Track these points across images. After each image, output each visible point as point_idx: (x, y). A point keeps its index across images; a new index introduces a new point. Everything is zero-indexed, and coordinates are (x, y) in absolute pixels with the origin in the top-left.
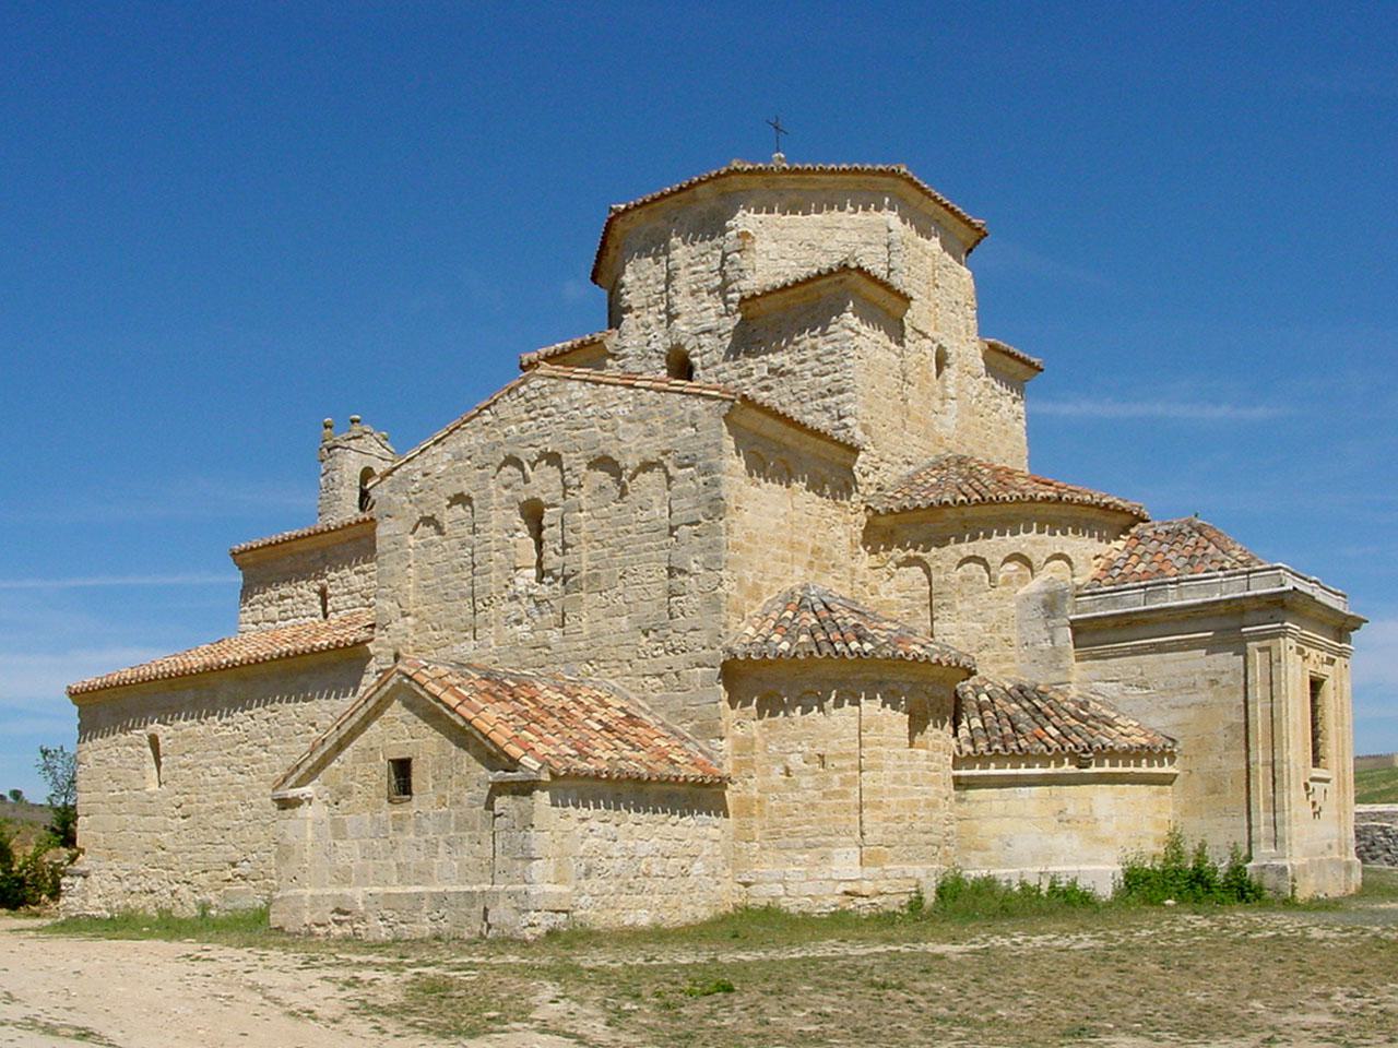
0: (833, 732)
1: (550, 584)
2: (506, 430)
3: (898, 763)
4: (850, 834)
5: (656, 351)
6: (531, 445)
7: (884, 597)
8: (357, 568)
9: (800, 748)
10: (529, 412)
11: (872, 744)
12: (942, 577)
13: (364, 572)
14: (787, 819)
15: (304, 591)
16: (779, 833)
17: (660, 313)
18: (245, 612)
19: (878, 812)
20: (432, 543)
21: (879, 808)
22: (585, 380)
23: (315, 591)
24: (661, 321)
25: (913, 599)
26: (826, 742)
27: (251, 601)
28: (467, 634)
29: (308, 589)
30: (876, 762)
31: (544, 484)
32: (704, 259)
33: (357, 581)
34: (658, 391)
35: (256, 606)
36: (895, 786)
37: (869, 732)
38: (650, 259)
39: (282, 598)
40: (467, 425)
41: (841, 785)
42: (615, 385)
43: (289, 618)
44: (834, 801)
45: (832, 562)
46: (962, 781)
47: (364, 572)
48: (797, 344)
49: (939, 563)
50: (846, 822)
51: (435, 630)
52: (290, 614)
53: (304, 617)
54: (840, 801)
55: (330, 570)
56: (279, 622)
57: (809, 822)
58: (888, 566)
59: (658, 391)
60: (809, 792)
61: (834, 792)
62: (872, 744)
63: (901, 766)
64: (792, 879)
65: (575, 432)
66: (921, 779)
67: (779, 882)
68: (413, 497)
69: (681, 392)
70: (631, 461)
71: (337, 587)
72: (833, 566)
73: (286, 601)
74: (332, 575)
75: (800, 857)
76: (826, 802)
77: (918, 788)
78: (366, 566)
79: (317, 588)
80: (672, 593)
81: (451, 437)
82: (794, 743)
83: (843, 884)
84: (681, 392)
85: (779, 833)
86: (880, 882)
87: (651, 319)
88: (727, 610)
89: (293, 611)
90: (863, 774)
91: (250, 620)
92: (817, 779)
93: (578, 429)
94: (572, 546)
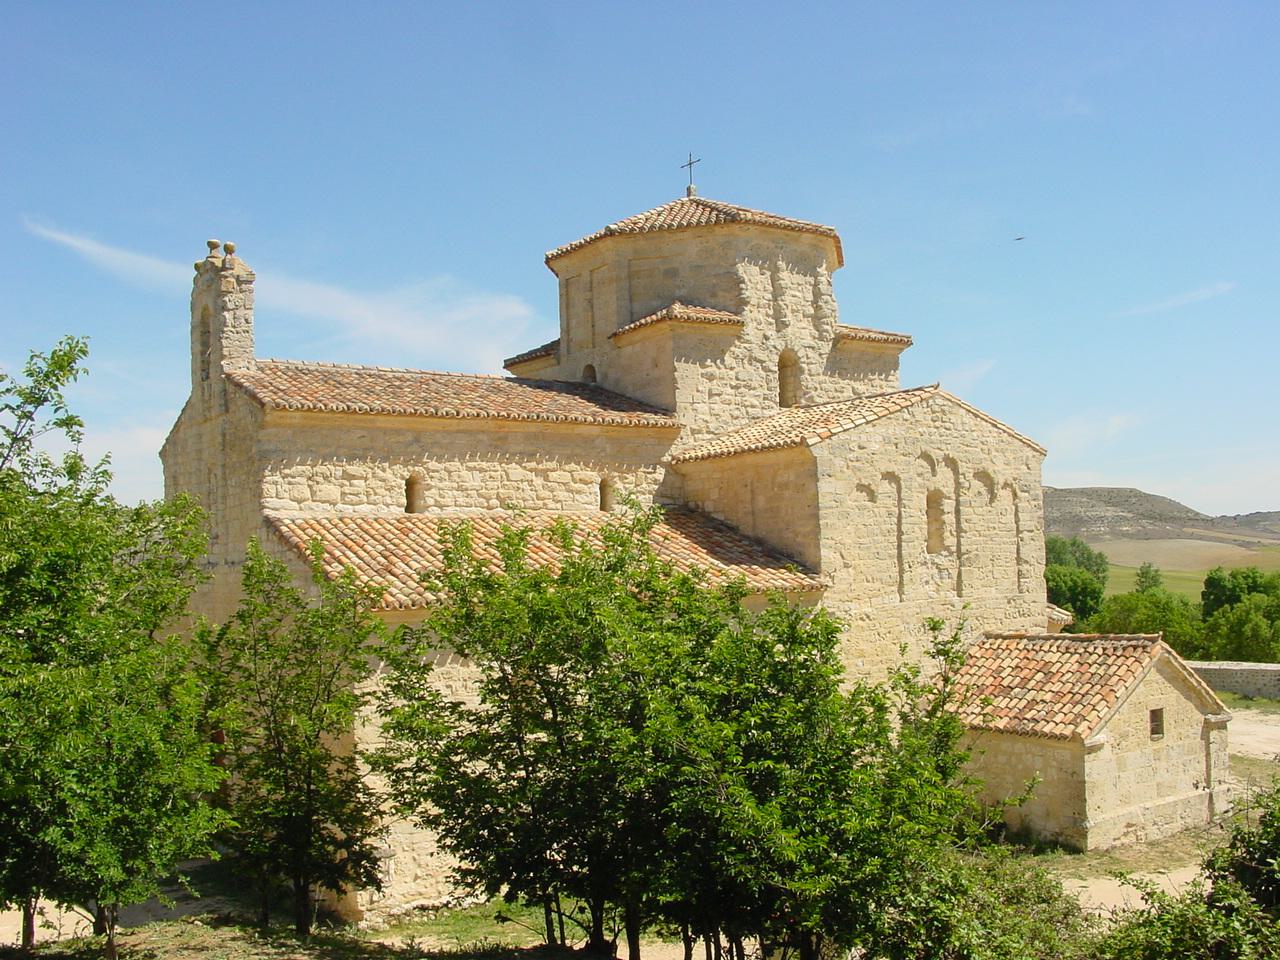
1: (946, 556)
2: (920, 430)
5: (775, 347)
6: (939, 449)
8: (471, 464)
10: (934, 421)
13: (481, 470)
15: (388, 475)
17: (768, 315)
18: (275, 483)
20: (865, 508)
22: (969, 411)
23: (402, 478)
24: (771, 324)
27: (287, 471)
28: (893, 588)
29: (396, 475)
31: (944, 479)
32: (800, 288)
33: (473, 480)
34: (1010, 435)
35: (298, 479)
38: (757, 268)
39: (350, 477)
40: (892, 416)
42: (987, 421)
43: (361, 503)
47: (481, 470)
48: (871, 380)
51: (868, 582)
52: (365, 499)
53: (388, 505)
55: (430, 458)
56: (340, 506)
59: (1010, 435)
65: (966, 448)
68: (850, 464)
69: (1021, 440)
70: (1000, 480)
71: (441, 480)
73: (355, 482)
74: (433, 464)
78: (484, 465)
79: (407, 475)
80: (1020, 574)
81: (879, 421)
84: (1021, 440)
87: (761, 317)
89: (368, 495)
91: (286, 495)
93: (967, 446)
94: (966, 532)
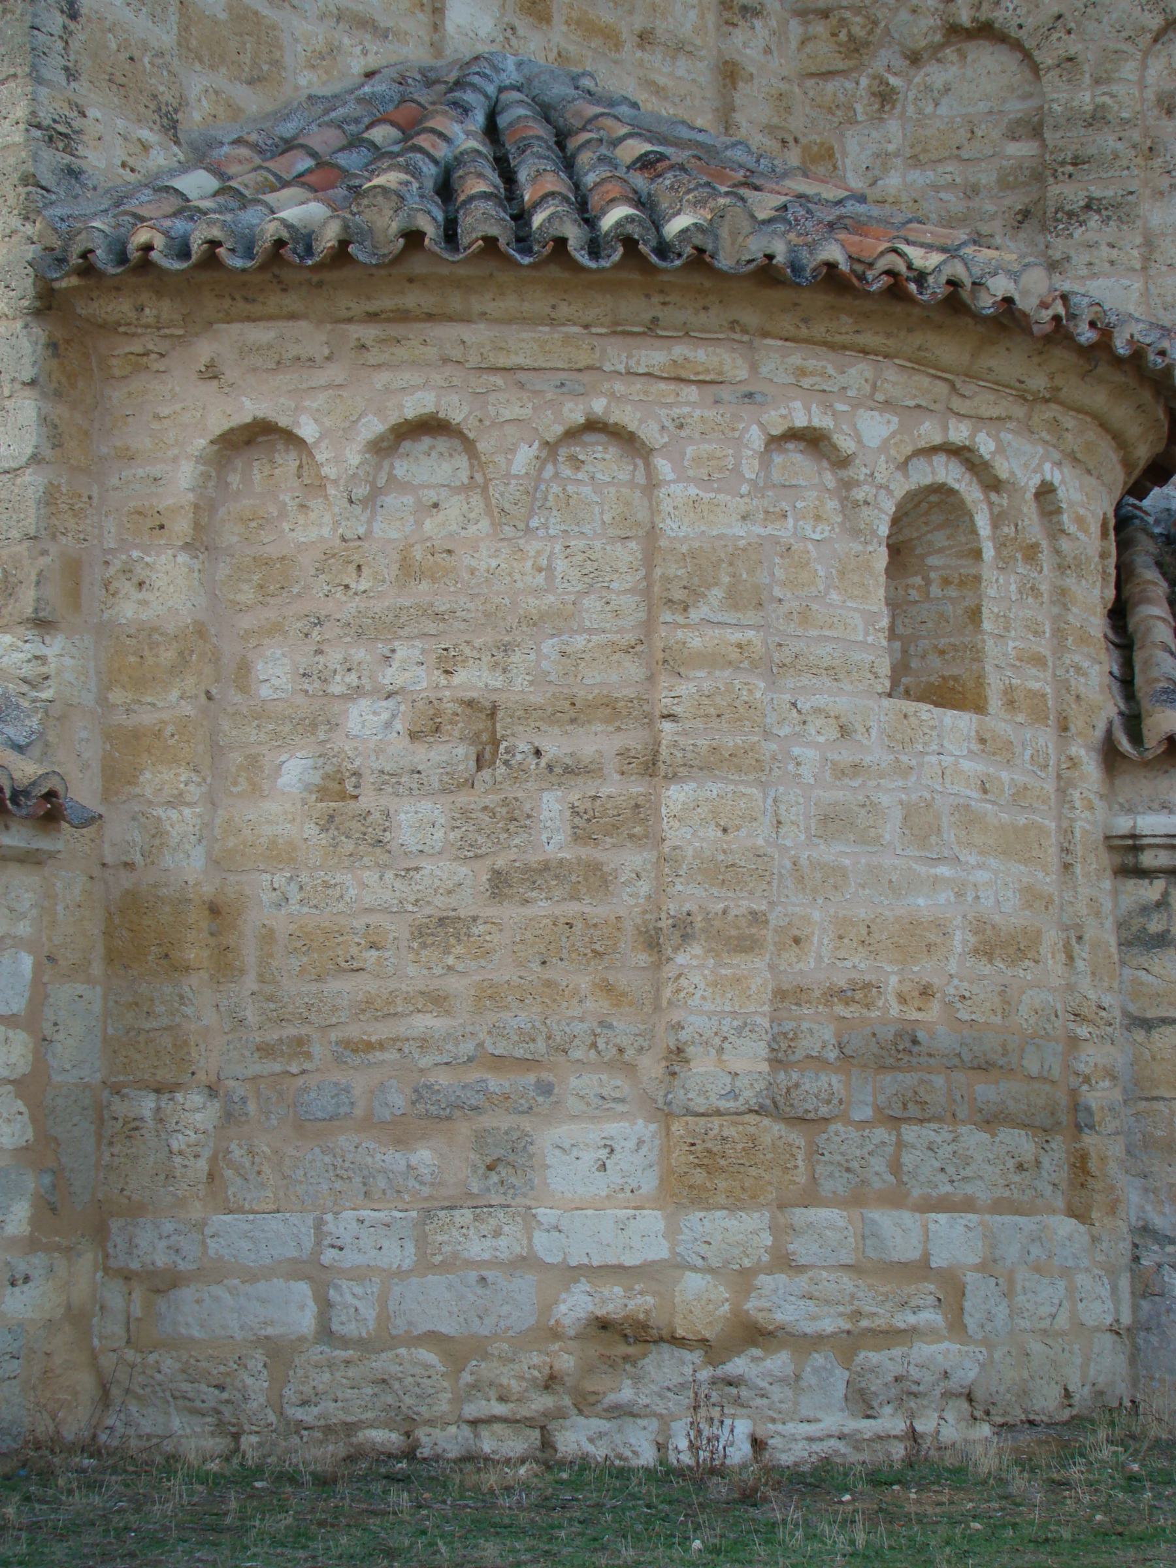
0: (531, 604)
3: (845, 755)
4: (621, 1063)
7: (856, 183)
9: (390, 676)
11: (712, 660)
12: (1085, 99)
14: (343, 988)
16: (300, 1045)
19: (742, 963)
21: (746, 945)
25: (972, 191)
26: (507, 648)
30: (731, 741)
36: (830, 852)
37: (694, 615)
41: (580, 837)
44: (542, 908)
45: (639, 22)
46: (1148, 859)
49: (1074, 46)
50: (597, 1005)
54: (572, 909)
57: (438, 1001)
58: (878, 66)
60: (428, 866)
61: (546, 867)
62: (712, 660)
63: (856, 768)
64: (350, 1259)
66: (950, 835)
67: (297, 1270)
72: (645, 38)
75: (394, 1159)
76: (511, 913)
77: (943, 870)
82: (360, 654)
83: (584, 1286)
85: (300, 1045)
86: (764, 1280)
88: (71, 74)
90: (676, 795)
92: (465, 813)
